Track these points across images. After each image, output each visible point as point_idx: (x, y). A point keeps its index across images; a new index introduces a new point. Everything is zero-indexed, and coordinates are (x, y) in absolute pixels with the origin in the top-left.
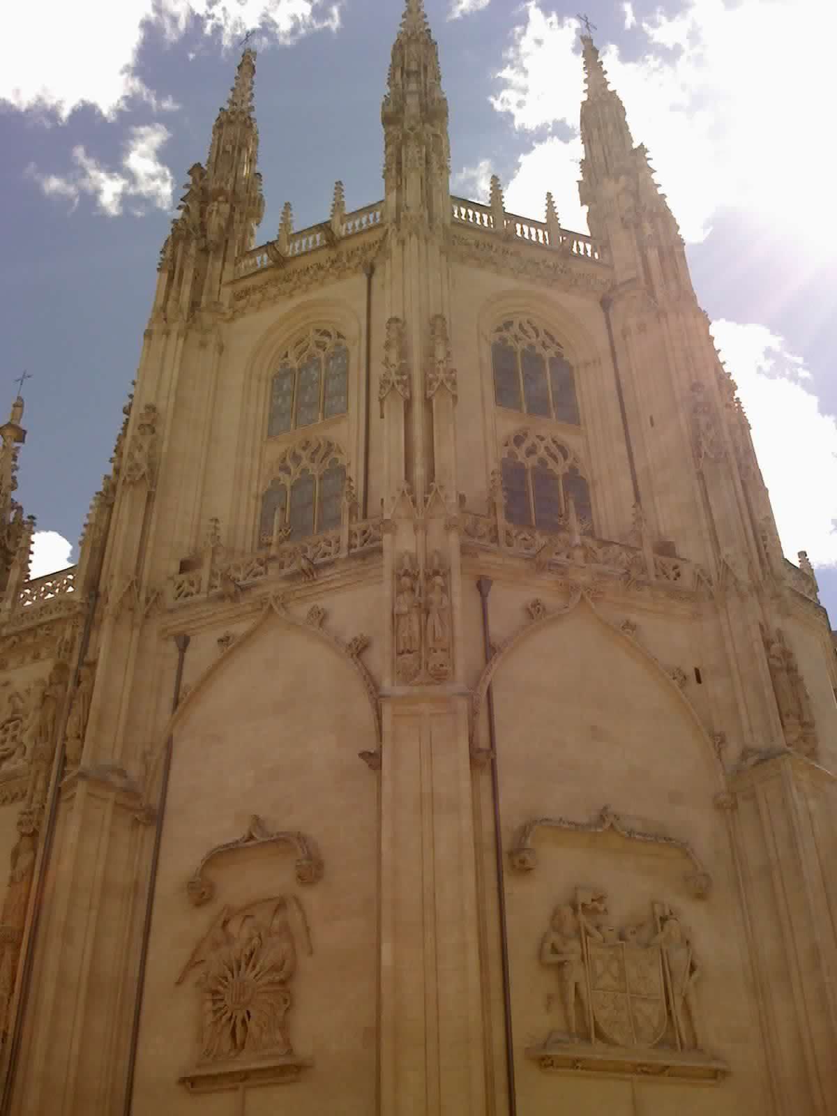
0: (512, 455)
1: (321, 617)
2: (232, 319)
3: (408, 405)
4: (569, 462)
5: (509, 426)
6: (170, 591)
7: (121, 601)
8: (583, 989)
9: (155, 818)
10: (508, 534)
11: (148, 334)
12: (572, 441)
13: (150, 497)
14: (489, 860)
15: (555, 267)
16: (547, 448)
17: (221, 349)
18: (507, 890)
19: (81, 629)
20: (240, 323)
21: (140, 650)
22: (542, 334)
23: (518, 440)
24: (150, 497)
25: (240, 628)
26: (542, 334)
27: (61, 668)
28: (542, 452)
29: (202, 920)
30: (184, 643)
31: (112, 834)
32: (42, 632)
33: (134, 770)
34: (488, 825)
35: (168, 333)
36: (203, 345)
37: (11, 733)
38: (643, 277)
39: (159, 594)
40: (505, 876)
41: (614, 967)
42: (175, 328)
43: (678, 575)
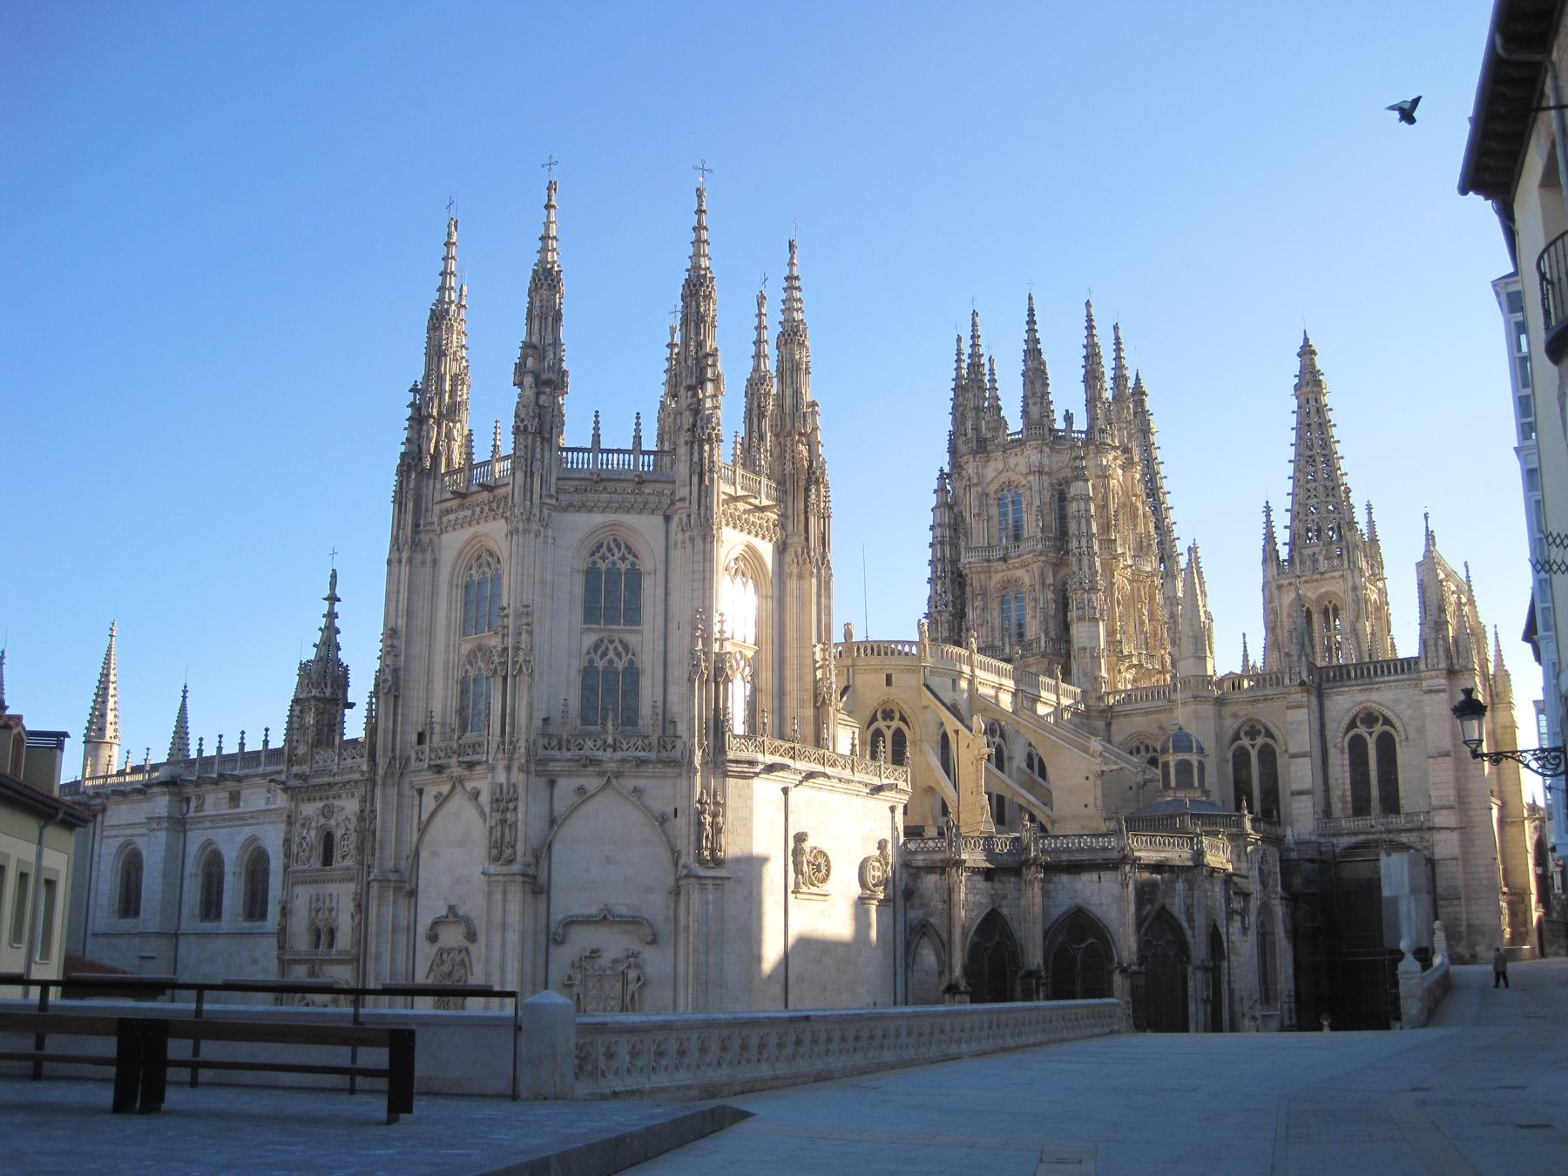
0: (591, 661)
1: (476, 795)
2: (442, 533)
3: (505, 678)
4: (629, 656)
5: (590, 639)
6: (413, 757)
7: (386, 773)
8: (581, 996)
9: (413, 893)
10: (568, 741)
11: (389, 562)
12: (632, 639)
13: (396, 697)
14: (542, 939)
15: (633, 492)
16: (615, 649)
17: (435, 562)
18: (551, 950)
19: (369, 787)
20: (445, 537)
21: (400, 795)
22: (623, 546)
23: (597, 646)
24: (396, 697)
25: (445, 789)
26: (623, 546)
27: (362, 811)
28: (611, 654)
29: (435, 948)
30: (420, 792)
31: (395, 903)
32: (352, 784)
33: (403, 865)
34: (544, 920)
35: (400, 561)
36: (423, 563)
37: (346, 843)
38: (688, 500)
39: (409, 757)
40: (551, 945)
41: (598, 985)
42: (405, 555)
43: (674, 747)
